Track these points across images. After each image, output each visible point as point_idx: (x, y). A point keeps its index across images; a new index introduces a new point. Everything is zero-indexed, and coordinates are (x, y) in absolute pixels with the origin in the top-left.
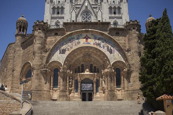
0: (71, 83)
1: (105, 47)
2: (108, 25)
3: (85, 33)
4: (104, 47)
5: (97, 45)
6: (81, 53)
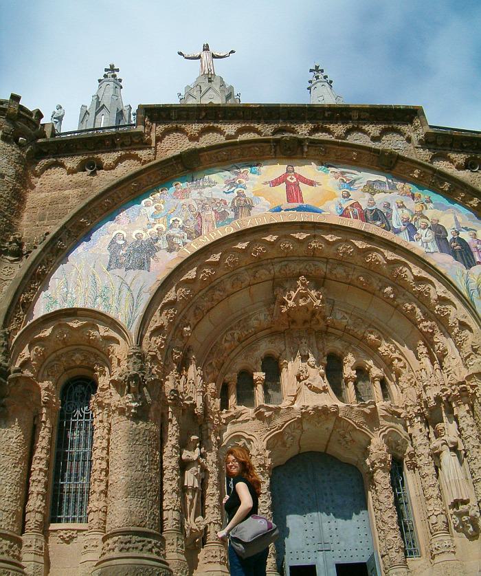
0: (191, 479)
3: (275, 158)
4: (412, 229)
5: (363, 216)
6: (263, 273)
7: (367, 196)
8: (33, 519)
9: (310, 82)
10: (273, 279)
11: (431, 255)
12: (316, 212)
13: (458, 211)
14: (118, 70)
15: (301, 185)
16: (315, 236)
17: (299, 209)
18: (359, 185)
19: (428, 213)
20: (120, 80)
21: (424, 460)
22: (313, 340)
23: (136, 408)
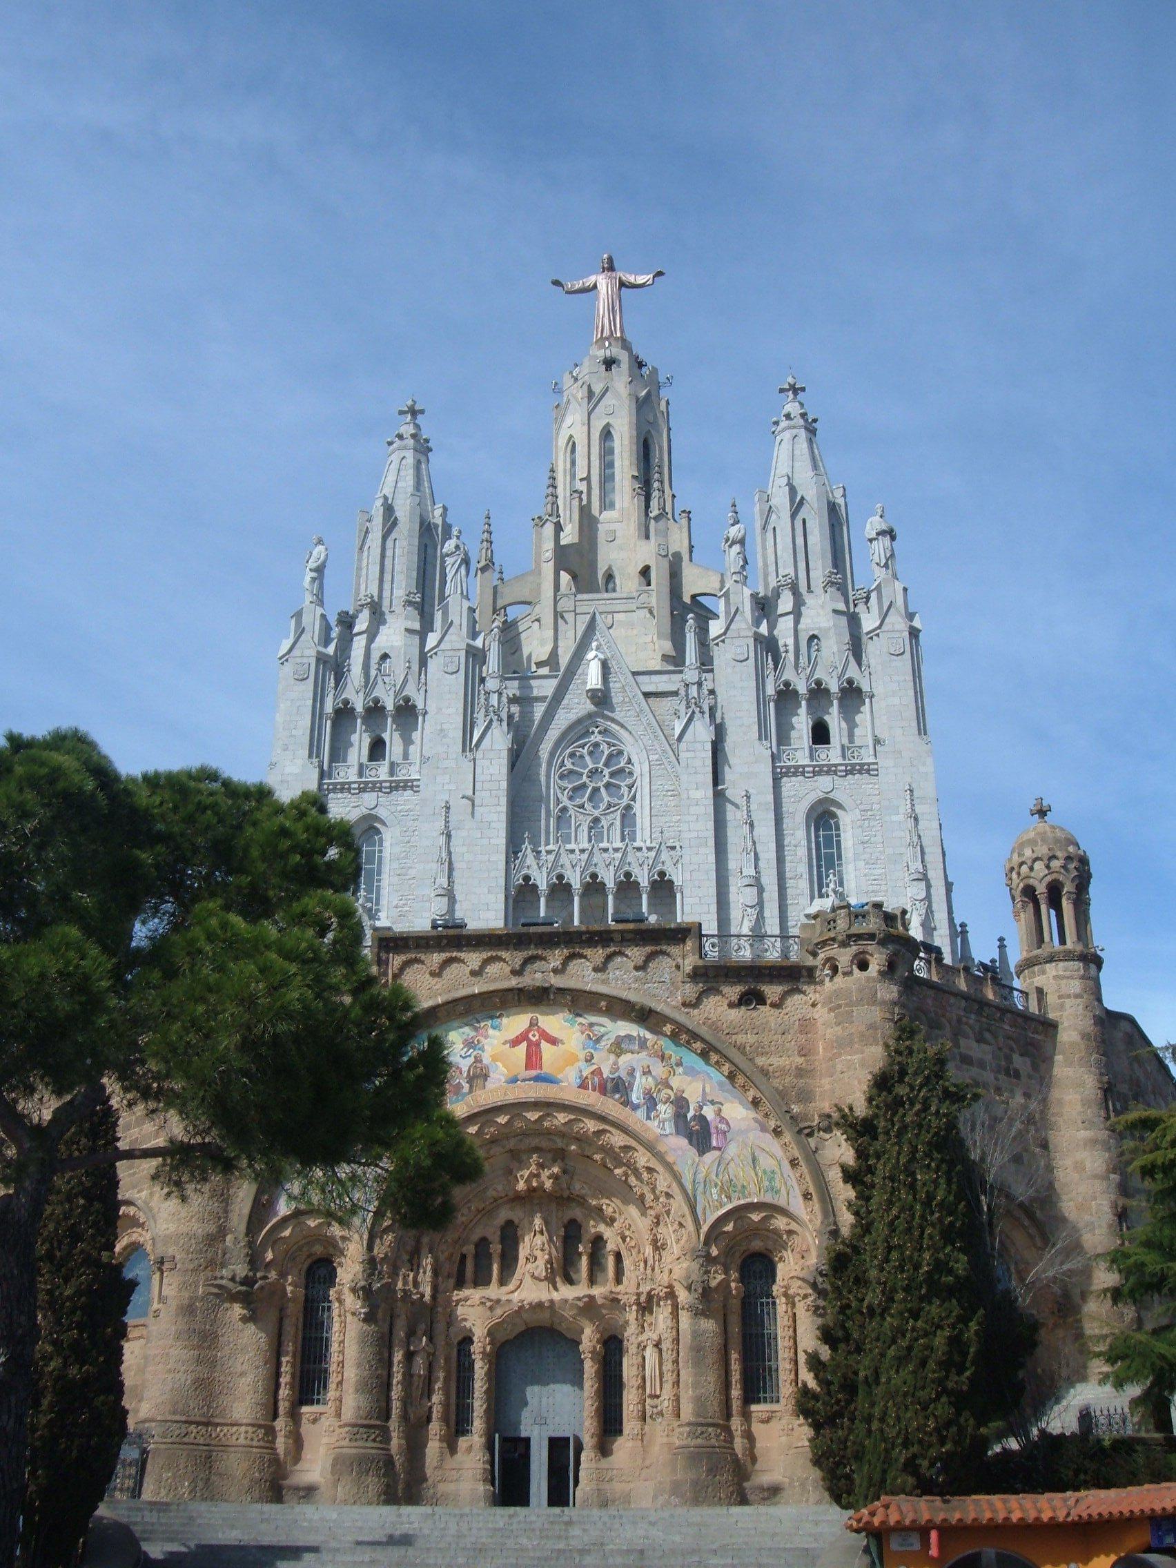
1: (661, 1107)
2: (683, 941)
5: (603, 1089)
6: (496, 1150)
7: (612, 1057)
8: (283, 1406)
9: (776, 423)
10: (510, 1151)
11: (665, 1139)
12: (552, 1082)
13: (708, 1075)
14: (422, 412)
15: (544, 1045)
16: (548, 1115)
17: (537, 1079)
18: (606, 1043)
19: (675, 1082)
20: (427, 441)
21: (632, 1349)
22: (554, 1206)
23: (364, 1313)
